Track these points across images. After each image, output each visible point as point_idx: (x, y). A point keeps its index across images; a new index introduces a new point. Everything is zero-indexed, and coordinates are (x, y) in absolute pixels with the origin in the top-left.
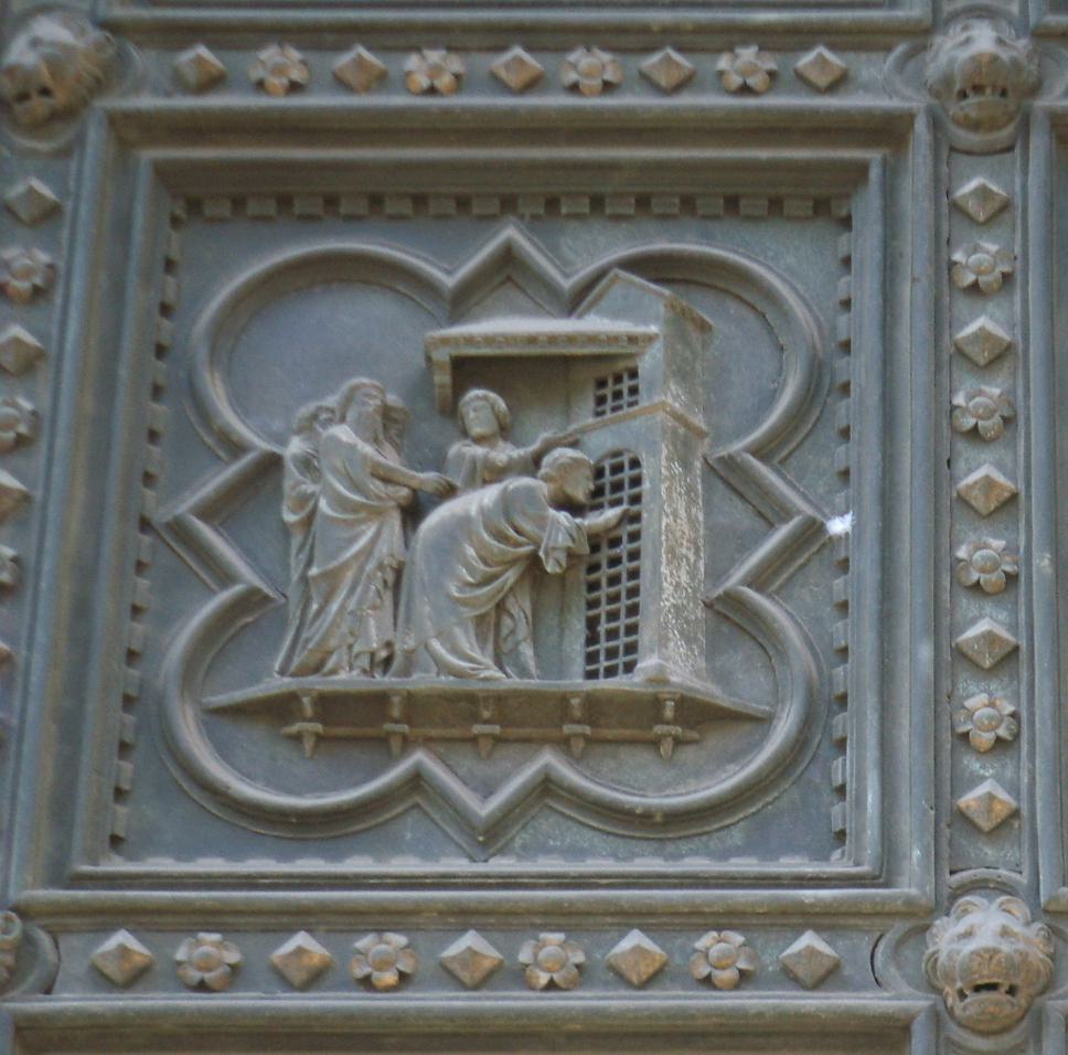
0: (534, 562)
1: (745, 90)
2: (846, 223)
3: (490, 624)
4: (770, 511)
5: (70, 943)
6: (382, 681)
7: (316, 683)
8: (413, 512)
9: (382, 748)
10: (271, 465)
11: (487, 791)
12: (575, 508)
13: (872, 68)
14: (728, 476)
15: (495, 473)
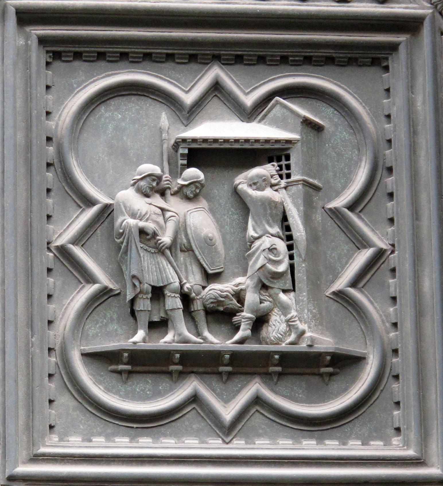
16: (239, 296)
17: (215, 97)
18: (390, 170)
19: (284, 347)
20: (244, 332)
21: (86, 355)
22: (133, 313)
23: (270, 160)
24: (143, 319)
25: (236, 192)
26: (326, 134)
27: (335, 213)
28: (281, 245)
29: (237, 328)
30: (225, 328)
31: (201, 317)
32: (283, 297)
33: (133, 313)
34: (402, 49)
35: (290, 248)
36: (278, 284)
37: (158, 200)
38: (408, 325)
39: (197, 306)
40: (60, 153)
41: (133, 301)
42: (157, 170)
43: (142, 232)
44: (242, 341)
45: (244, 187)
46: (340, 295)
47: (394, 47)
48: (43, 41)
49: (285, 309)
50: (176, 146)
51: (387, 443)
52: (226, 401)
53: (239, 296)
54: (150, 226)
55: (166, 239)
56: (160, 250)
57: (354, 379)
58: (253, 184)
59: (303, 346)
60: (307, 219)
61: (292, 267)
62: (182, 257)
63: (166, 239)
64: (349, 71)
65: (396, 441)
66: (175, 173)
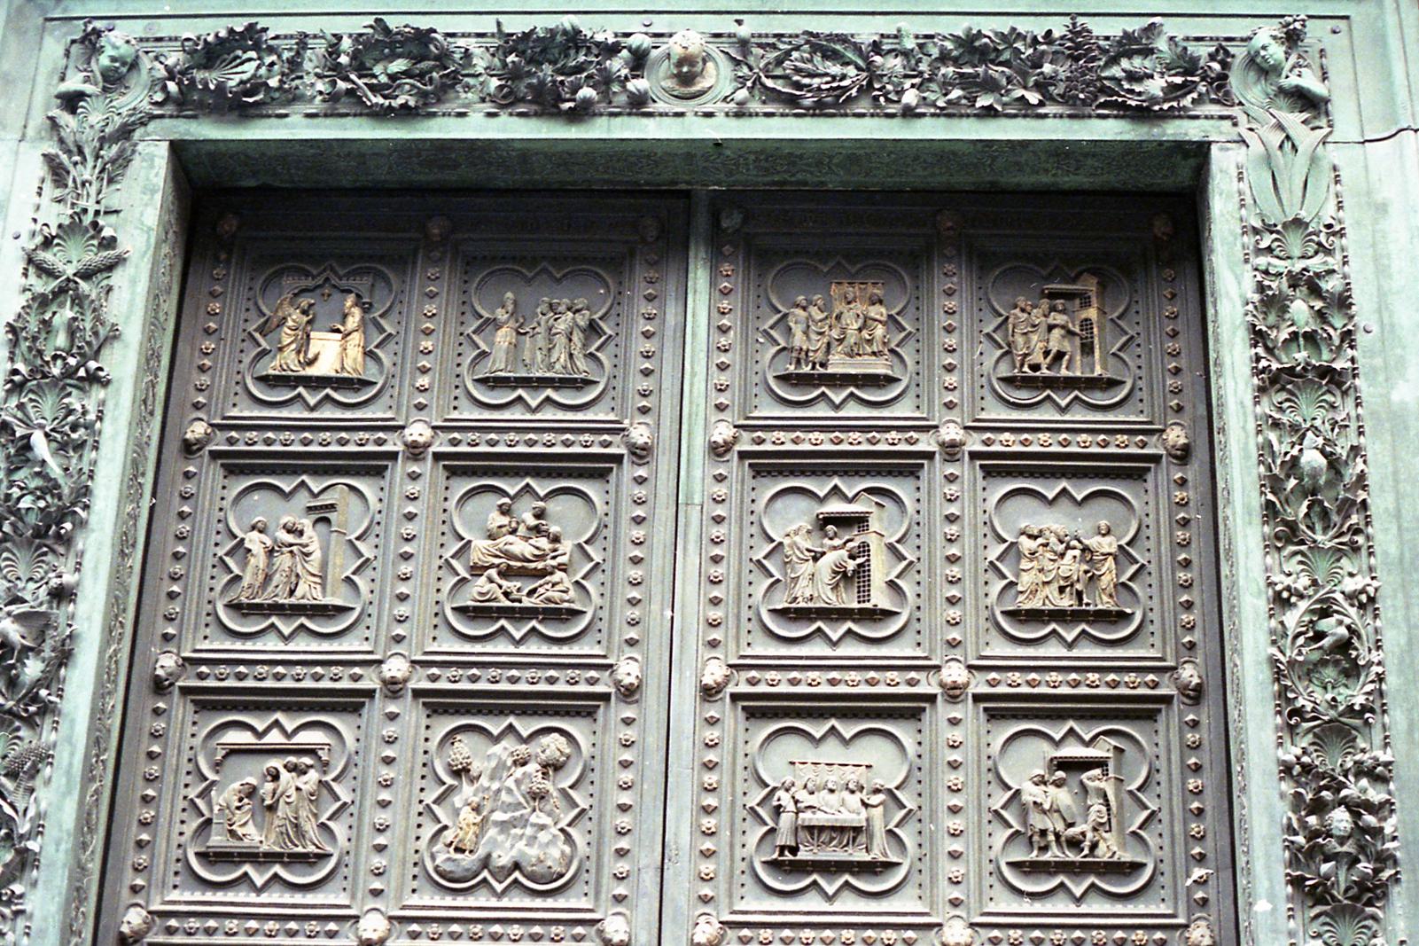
0: (845, 573)
1: (893, 444)
2: (918, 478)
3: (835, 588)
4: (901, 558)
5: (742, 673)
6: (810, 605)
7: (794, 605)
8: (815, 559)
9: (813, 621)
10: (781, 544)
11: (835, 631)
12: (852, 557)
13: (923, 437)
14: (891, 547)
15: (835, 548)
16: (1083, 834)
17: (1071, 740)
18: (1158, 771)
19: (1105, 859)
20: (1086, 851)
21: (1008, 863)
22: (1031, 843)
23: (1098, 767)
24: (1036, 846)
25: (1081, 783)
26: (1127, 753)
27: (1131, 792)
28: (1104, 809)
29: (1082, 850)
30: (1075, 851)
31: (1064, 845)
32: (1104, 835)
33: (1031, 843)
34: (1164, 713)
35: (1108, 810)
36: (1101, 829)
37: (1043, 787)
38: (1167, 848)
39: (1063, 839)
40: (995, 764)
41: (1031, 837)
42: (1042, 773)
43: (1035, 803)
44: (1085, 856)
45: (1085, 781)
46: (1134, 833)
47: (1159, 711)
48: (986, 709)
49: (1105, 840)
50: (1052, 760)
51: (1158, 907)
52: (1078, 885)
53: (1083, 834)
54: (1039, 801)
55: (1047, 806)
56: (1044, 812)
57: (1140, 876)
58: (1089, 779)
59: (1115, 859)
60: (1117, 796)
61: (1109, 820)
62: (1056, 815)
63: (1047, 806)
64: (1137, 722)
65: (1162, 905)
66: (1052, 773)
